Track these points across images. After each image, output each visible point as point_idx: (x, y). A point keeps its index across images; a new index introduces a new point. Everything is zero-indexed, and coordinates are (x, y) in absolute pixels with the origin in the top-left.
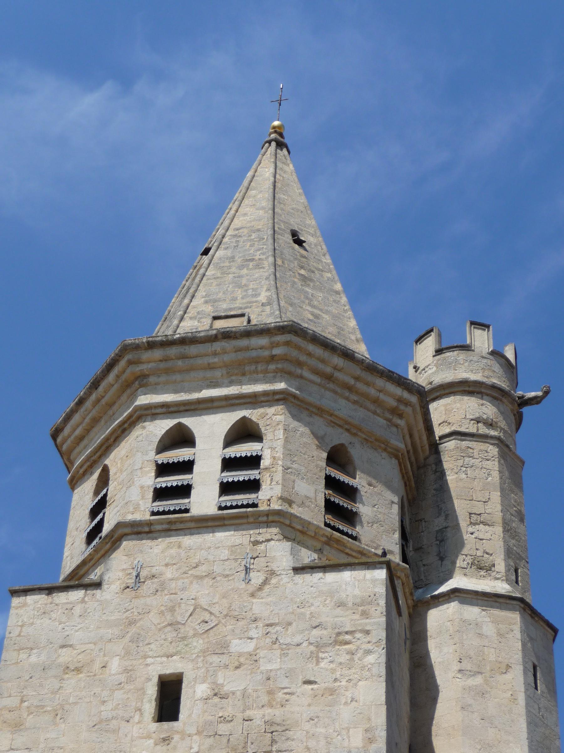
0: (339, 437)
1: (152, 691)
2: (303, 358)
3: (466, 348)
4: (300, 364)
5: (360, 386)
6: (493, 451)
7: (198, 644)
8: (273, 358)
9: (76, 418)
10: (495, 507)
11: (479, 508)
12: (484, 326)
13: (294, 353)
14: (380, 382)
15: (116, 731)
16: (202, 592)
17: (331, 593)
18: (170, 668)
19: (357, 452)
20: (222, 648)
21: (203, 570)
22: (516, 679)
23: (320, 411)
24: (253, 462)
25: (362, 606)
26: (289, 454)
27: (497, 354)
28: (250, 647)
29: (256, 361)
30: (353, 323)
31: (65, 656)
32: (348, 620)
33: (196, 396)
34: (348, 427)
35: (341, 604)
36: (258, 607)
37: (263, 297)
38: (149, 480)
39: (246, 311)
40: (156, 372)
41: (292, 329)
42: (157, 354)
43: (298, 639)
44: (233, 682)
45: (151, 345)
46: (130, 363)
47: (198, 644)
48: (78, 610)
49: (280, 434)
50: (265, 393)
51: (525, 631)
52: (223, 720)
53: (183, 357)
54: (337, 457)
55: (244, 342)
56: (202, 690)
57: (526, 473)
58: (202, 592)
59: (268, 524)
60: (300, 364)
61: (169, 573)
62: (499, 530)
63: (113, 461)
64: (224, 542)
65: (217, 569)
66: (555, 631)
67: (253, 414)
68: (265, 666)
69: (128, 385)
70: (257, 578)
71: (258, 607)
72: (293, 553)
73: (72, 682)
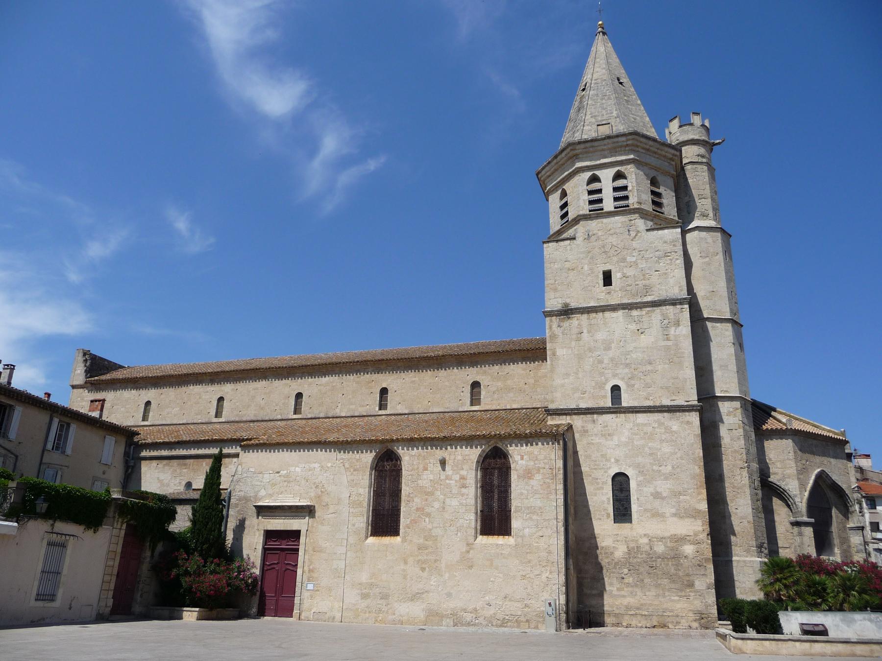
0: (653, 173)
1: (601, 276)
2: (639, 144)
3: (692, 124)
4: (637, 146)
5: (659, 152)
6: (705, 168)
7: (615, 259)
8: (627, 145)
9: (547, 168)
10: (708, 192)
11: (702, 192)
12: (697, 114)
13: (635, 142)
14: (666, 149)
15: (591, 291)
16: (613, 240)
17: (661, 238)
18: (607, 268)
19: (660, 178)
20: (624, 260)
21: (612, 231)
22: (720, 257)
23: (646, 164)
24: (625, 188)
25: (673, 242)
26: (638, 184)
27: (703, 125)
28: (634, 259)
29: (621, 147)
30: (648, 119)
31: (567, 265)
32: (669, 248)
33: (598, 162)
34: (656, 169)
35: (665, 242)
36: (635, 244)
37: (615, 114)
38: (586, 197)
39: (609, 121)
40: (581, 153)
41: (635, 133)
42: (582, 146)
43: (651, 255)
44: (630, 272)
45: (580, 143)
46: (572, 150)
47: (615, 259)
48: (568, 248)
49: (634, 176)
50: (626, 160)
51: (722, 239)
52: (628, 285)
53: (592, 147)
54: (654, 182)
55: (616, 140)
56: (619, 275)
57: (716, 173)
58: (613, 240)
59: (634, 213)
60: (637, 146)
61: (600, 233)
62: (710, 200)
63: (567, 187)
65: (618, 231)
66: (730, 236)
67: (622, 168)
68: (640, 266)
69: (571, 158)
70: (633, 234)
73: (571, 274)
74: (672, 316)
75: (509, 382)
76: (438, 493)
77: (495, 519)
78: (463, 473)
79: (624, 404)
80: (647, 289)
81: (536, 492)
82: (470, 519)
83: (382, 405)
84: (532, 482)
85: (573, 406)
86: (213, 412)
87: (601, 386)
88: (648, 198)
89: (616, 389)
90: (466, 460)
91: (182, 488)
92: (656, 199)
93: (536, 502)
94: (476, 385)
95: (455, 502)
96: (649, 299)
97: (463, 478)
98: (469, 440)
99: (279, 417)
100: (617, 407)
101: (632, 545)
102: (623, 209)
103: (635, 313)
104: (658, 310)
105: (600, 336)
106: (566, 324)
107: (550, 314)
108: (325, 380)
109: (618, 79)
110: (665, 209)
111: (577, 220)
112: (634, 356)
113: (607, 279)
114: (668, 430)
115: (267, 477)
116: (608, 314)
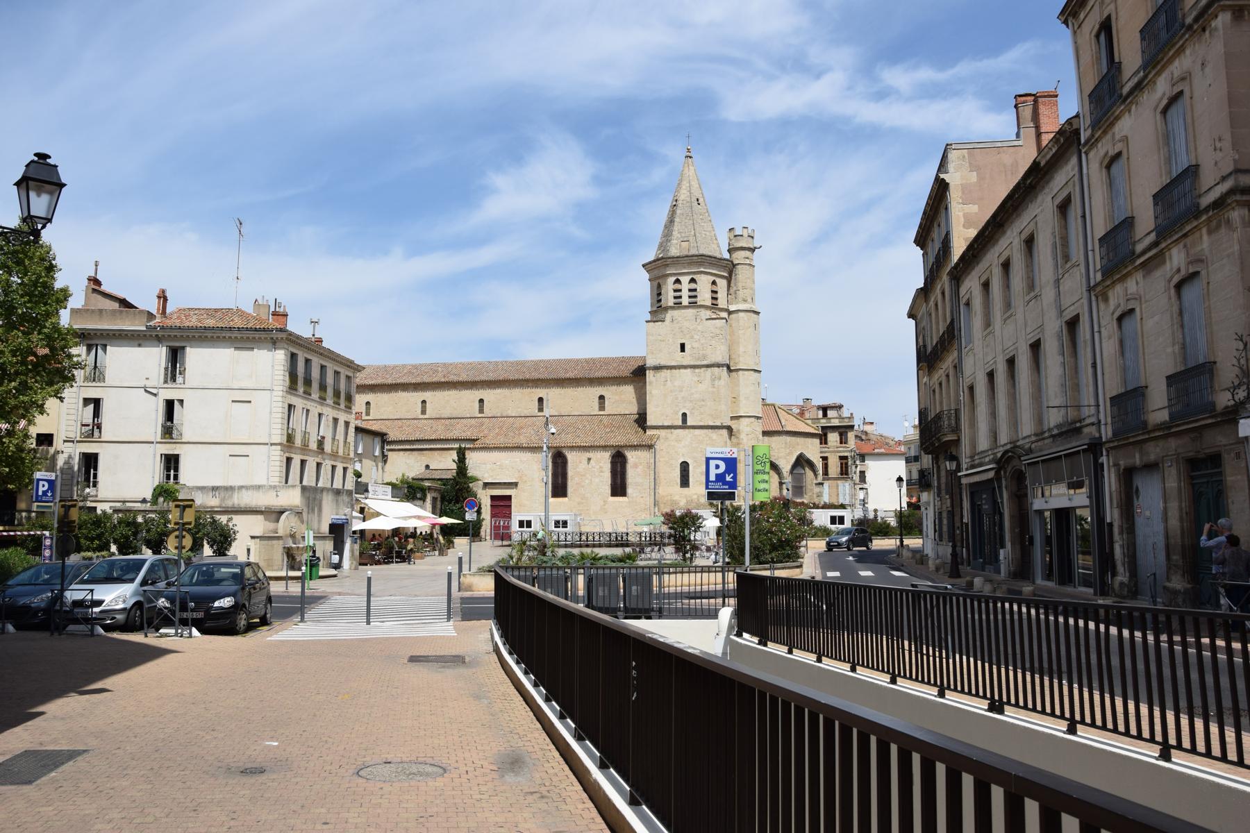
38: (671, 294)
44: (696, 345)
64: (691, 312)
77: (619, 488)
80: (704, 357)
82: (607, 489)
83: (541, 410)
88: (708, 295)
89: (684, 415)
90: (603, 461)
91: (423, 468)
94: (602, 398)
98: (604, 448)
100: (684, 425)
105: (676, 383)
107: (650, 368)
108: (498, 391)
110: (719, 301)
111: (667, 309)
113: (683, 347)
115: (488, 466)
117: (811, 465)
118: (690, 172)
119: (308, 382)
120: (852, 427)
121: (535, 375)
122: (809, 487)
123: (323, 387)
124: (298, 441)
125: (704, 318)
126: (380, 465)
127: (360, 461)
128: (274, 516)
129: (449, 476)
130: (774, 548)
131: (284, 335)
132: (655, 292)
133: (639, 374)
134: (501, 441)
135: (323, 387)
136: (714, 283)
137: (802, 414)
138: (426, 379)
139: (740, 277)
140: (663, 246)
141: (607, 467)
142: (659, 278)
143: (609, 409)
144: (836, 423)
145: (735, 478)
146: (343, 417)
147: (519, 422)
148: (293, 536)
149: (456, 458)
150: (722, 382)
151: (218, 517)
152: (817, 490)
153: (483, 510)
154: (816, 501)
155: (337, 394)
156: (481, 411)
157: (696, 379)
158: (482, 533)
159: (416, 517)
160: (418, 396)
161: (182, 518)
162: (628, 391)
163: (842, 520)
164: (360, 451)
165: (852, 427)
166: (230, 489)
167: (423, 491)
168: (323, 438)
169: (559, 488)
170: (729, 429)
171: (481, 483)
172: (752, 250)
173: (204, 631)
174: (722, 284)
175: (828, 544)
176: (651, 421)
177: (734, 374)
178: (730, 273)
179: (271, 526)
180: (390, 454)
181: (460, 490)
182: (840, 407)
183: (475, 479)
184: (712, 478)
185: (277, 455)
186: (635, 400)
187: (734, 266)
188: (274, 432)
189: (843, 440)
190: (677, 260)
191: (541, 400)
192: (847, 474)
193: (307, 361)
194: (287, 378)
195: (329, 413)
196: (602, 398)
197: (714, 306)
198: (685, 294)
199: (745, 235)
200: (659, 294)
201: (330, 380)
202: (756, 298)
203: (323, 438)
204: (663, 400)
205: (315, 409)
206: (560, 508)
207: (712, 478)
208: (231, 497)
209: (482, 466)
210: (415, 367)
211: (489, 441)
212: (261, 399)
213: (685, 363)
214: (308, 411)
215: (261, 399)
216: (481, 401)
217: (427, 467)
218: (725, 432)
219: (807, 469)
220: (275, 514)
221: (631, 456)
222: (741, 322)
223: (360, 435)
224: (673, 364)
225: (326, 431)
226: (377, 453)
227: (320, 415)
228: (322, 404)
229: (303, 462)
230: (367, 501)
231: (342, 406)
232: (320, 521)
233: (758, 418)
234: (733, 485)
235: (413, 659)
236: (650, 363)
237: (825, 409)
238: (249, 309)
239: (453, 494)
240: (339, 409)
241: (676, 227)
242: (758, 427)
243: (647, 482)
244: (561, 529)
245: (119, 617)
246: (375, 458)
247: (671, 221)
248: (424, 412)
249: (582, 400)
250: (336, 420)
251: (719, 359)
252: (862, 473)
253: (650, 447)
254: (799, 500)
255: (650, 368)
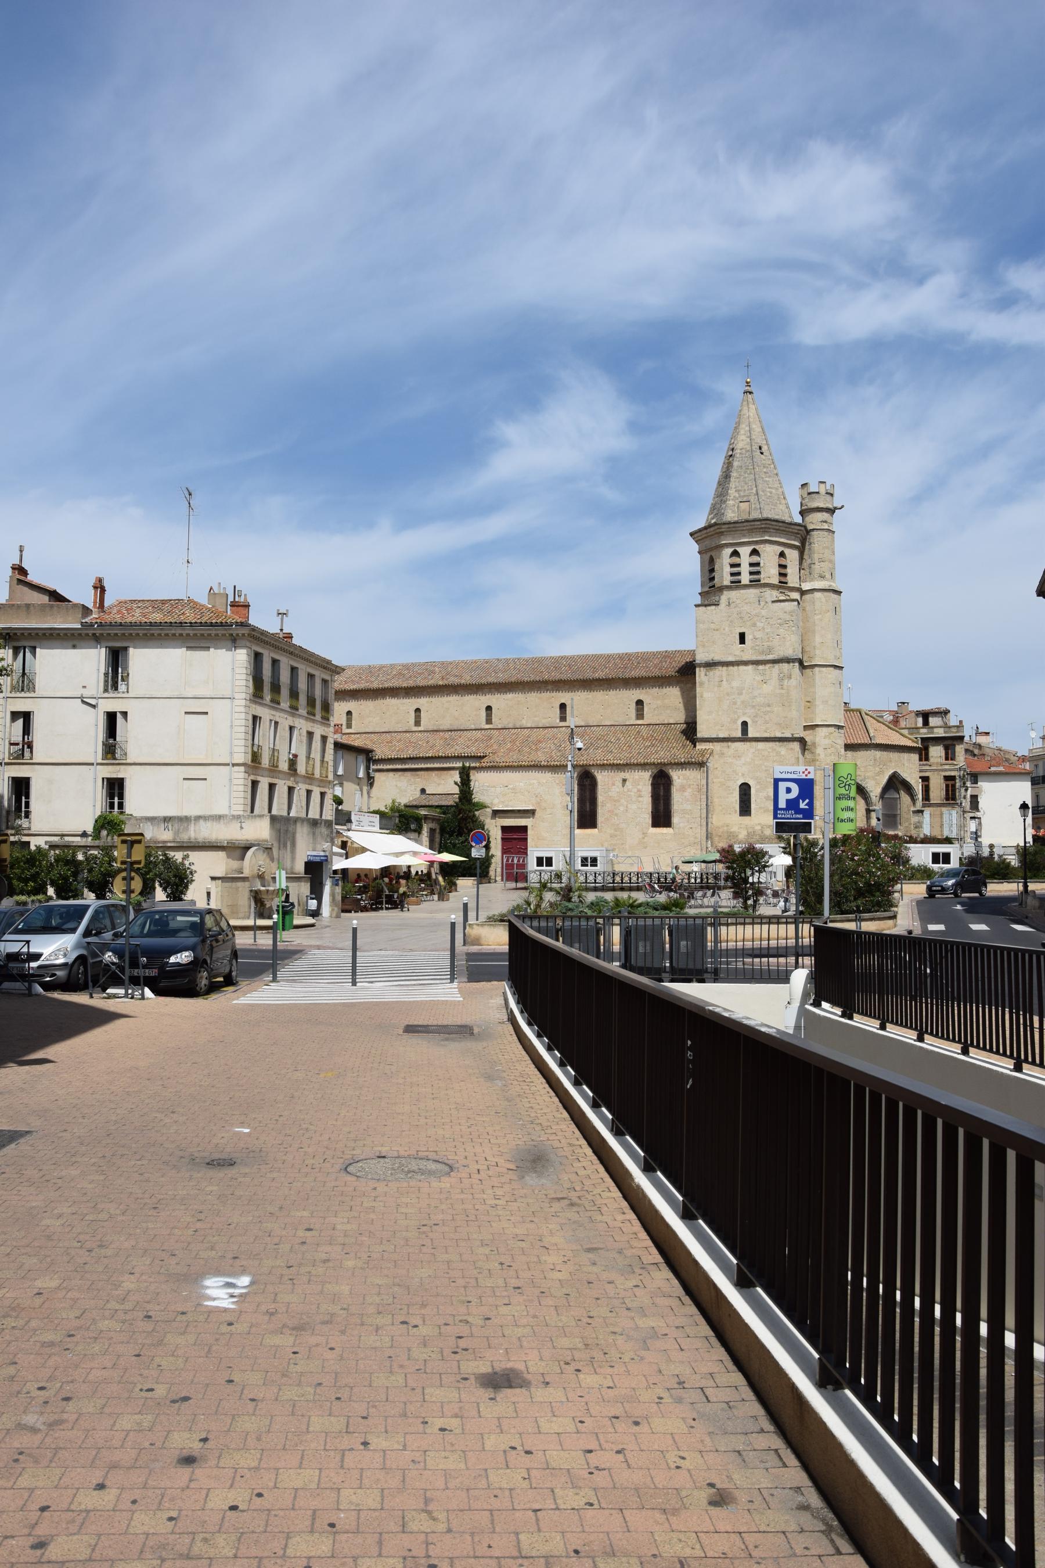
1: (738, 637)
7: (748, 623)
11: (821, 556)
16: (747, 608)
20: (754, 625)
24: (758, 564)
25: (791, 613)
28: (762, 625)
31: (713, 626)
32: (788, 617)
38: (727, 570)
44: (759, 635)
47: (748, 623)
58: (747, 608)
61: (738, 602)
64: (753, 592)
67: (757, 547)
71: (764, 612)
72: (771, 595)
74: (786, 671)
75: (666, 701)
76: (623, 801)
77: (662, 817)
78: (640, 787)
79: (750, 735)
80: (770, 650)
81: (688, 800)
83: (563, 718)
84: (686, 794)
85: (714, 736)
86: (412, 721)
87: (735, 721)
89: (745, 724)
91: (418, 793)
92: (783, 571)
93: (688, 807)
94: (640, 703)
95: (634, 807)
96: (770, 657)
97: (639, 791)
98: (643, 766)
99: (473, 727)
100: (744, 736)
101: (750, 830)
102: (755, 583)
103: (761, 667)
104: (777, 666)
105: (735, 684)
106: (711, 673)
107: (701, 665)
108: (510, 696)
109: (760, 448)
111: (722, 589)
112: (758, 700)
113: (742, 638)
114: (778, 754)
116: (742, 668)
117: (908, 788)
118: (750, 412)
119: (276, 688)
120: (962, 738)
121: (556, 676)
122: (904, 815)
123: (294, 694)
124: (265, 761)
125: (769, 600)
126: (365, 788)
127: (341, 785)
128: (238, 853)
129: (450, 802)
130: (860, 894)
131: (245, 631)
132: (707, 568)
133: (686, 673)
134: (513, 758)
135: (294, 694)
136: (782, 555)
137: (896, 721)
138: (421, 682)
139: (816, 546)
140: (716, 508)
141: (647, 790)
142: (711, 549)
143: (649, 717)
144: (940, 733)
145: (811, 804)
146: (319, 731)
147: (536, 734)
148: (261, 877)
149: (458, 780)
150: (793, 682)
151: (171, 854)
152: (915, 819)
153: (492, 845)
154: (914, 833)
155: (311, 702)
156: (489, 720)
157: (759, 678)
158: (492, 873)
159: (411, 853)
160: (408, 705)
161: (129, 855)
162: (673, 695)
163: (946, 858)
164: (340, 772)
165: (962, 738)
166: (185, 820)
167: (419, 820)
168: (295, 756)
169: (587, 817)
170: (802, 741)
171: (489, 810)
172: (832, 511)
173: (158, 992)
174: (792, 555)
175: (929, 889)
176: (702, 731)
177: (808, 670)
178: (803, 542)
179: (235, 864)
180: (377, 775)
181: (464, 819)
182: (946, 712)
183: (482, 806)
184: (782, 804)
185: (240, 778)
186: (681, 706)
187: (808, 532)
188: (236, 749)
189: (950, 756)
190: (734, 526)
191: (563, 707)
192: (954, 799)
193: (275, 662)
194: (251, 684)
195: (303, 725)
196: (640, 703)
197: (782, 585)
198: (745, 569)
199: (823, 491)
200: (712, 571)
201: (302, 685)
202: (837, 574)
203: (295, 756)
204: (717, 706)
205: (285, 721)
206: (588, 843)
207: (782, 804)
208: (187, 829)
209: (493, 790)
210: (406, 667)
211: (500, 759)
212: (219, 710)
213: (745, 658)
214: (276, 723)
215: (219, 710)
216: (489, 709)
217: (423, 791)
218: (796, 746)
219: (902, 793)
220: (239, 850)
221: (678, 777)
222: (818, 604)
223: (340, 753)
224: (731, 659)
225: (299, 747)
226: (361, 775)
227: (291, 728)
228: (293, 715)
229: (272, 787)
230: (350, 834)
231: (318, 717)
232: (293, 859)
233: (839, 727)
234: (809, 813)
235: (410, 1029)
236: (701, 657)
237: (926, 716)
238: (203, 599)
239: (454, 823)
240: (314, 721)
241: (733, 484)
242: (839, 739)
243: (697, 809)
244: (589, 868)
245: (59, 973)
246: (358, 781)
247: (726, 476)
248: (418, 723)
249: (613, 707)
250: (310, 735)
251: (789, 653)
252: (974, 799)
253: (701, 765)
254: (891, 833)
255: (701, 665)
